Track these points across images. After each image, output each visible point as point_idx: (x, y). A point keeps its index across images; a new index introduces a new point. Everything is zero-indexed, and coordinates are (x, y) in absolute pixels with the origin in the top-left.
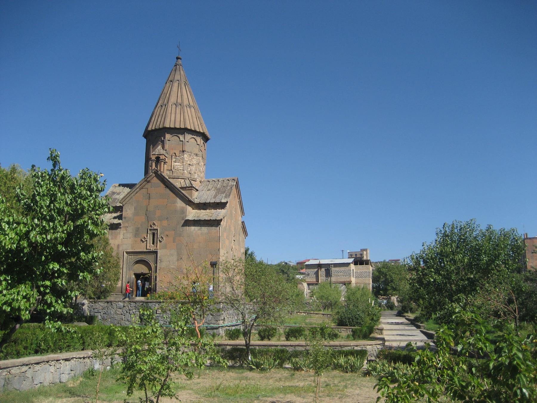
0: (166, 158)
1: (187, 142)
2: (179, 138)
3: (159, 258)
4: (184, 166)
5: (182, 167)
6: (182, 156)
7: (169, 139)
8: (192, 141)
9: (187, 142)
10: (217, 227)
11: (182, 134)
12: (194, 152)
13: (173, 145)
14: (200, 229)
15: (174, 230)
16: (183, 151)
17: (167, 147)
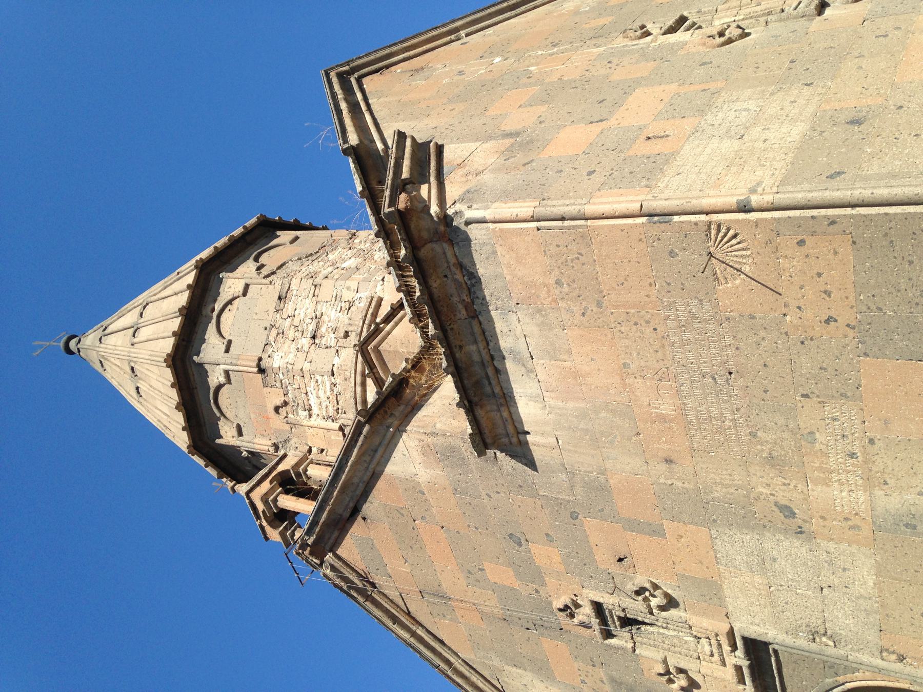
0: (281, 468)
1: (227, 351)
2: (219, 387)
3: (797, 637)
4: (313, 367)
5: (318, 377)
6: (281, 375)
7: (235, 433)
8: (230, 321)
9: (227, 351)
10: (467, 240)
11: (205, 374)
12: (272, 310)
13: (252, 416)
14: (519, 360)
15: (574, 516)
16: (261, 371)
17: (262, 444)
